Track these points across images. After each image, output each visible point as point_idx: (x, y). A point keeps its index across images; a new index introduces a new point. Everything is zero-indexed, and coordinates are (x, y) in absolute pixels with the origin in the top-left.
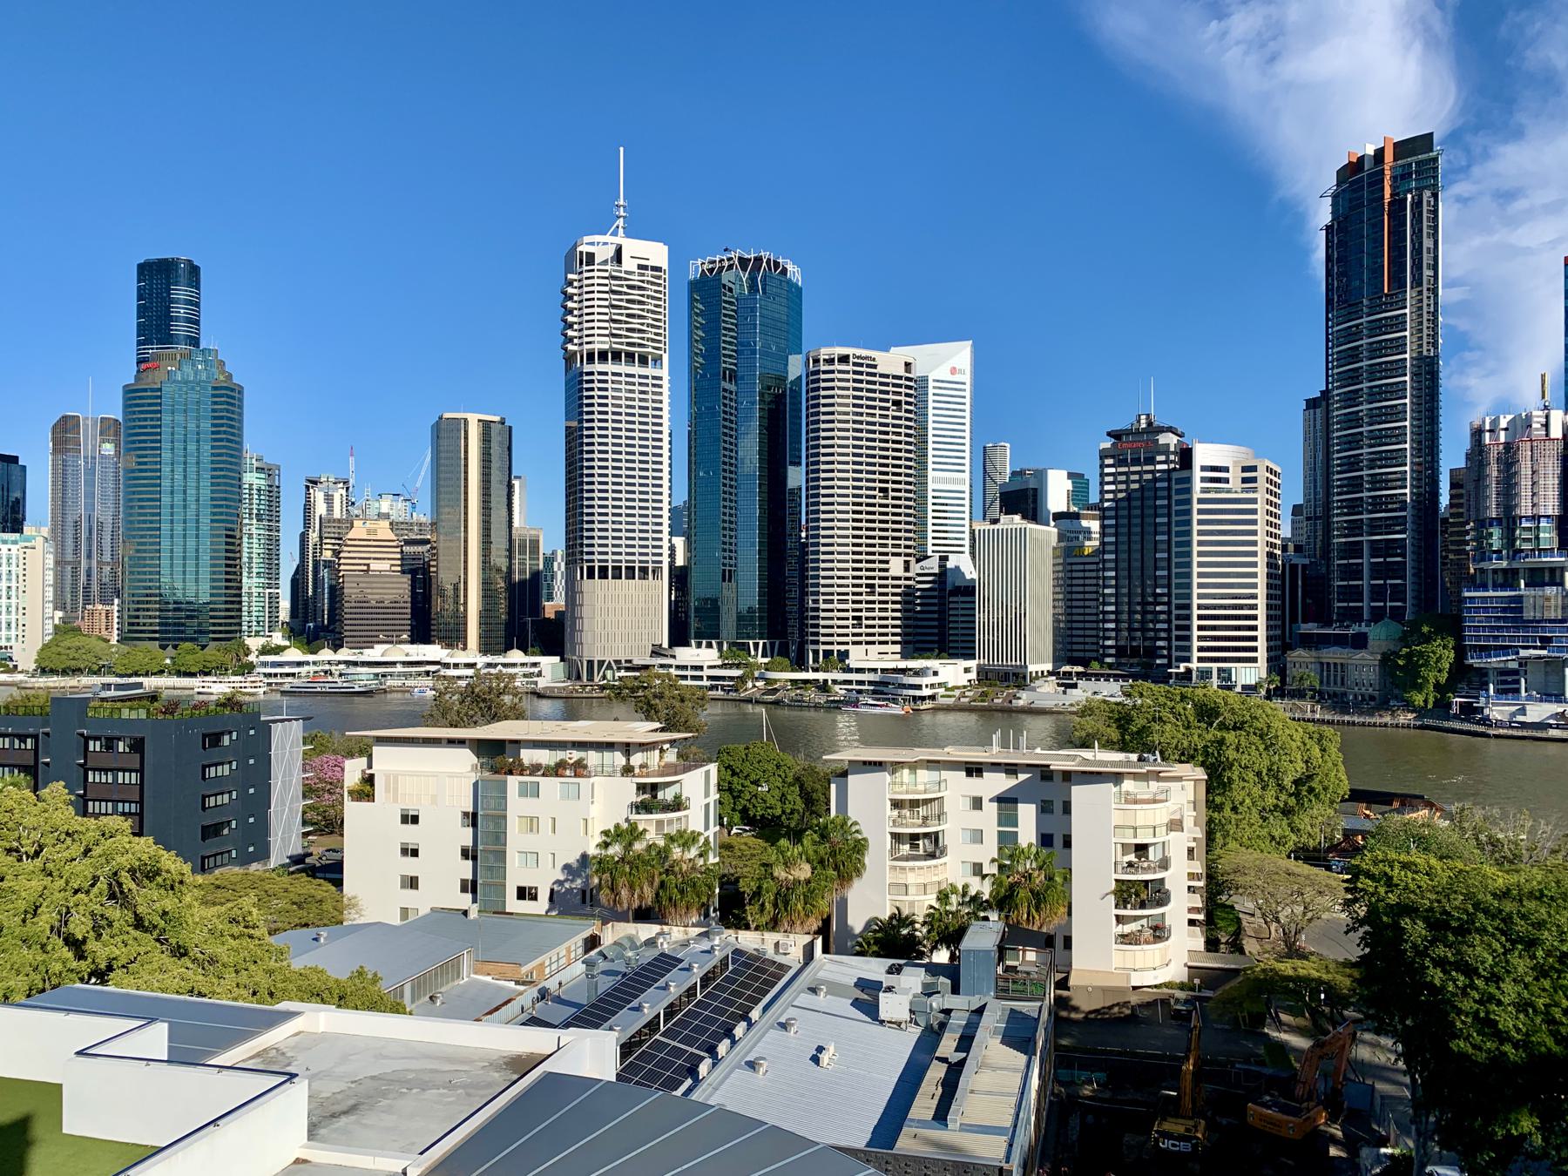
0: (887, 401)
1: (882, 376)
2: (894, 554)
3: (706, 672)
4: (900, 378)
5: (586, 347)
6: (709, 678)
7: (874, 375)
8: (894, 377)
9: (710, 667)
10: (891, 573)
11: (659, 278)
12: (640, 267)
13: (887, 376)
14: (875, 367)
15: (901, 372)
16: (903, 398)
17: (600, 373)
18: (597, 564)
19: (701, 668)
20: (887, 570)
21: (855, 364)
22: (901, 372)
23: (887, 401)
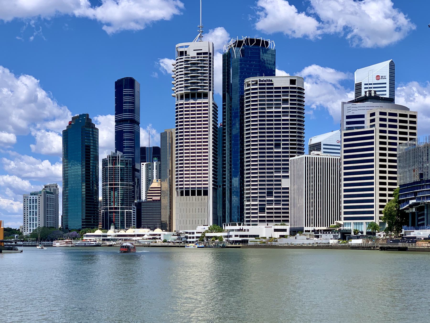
0: (280, 100)
1: (276, 88)
2: (284, 177)
3: (196, 235)
4: (287, 88)
5: (177, 93)
6: (197, 237)
7: (272, 88)
8: (284, 88)
9: (197, 233)
10: (283, 186)
11: (206, 57)
12: (198, 54)
13: (279, 88)
14: (272, 84)
15: (288, 85)
16: (289, 98)
17: (180, 104)
18: (184, 190)
19: (193, 233)
20: (280, 185)
21: (260, 84)
22: (288, 85)
23: (280, 100)
